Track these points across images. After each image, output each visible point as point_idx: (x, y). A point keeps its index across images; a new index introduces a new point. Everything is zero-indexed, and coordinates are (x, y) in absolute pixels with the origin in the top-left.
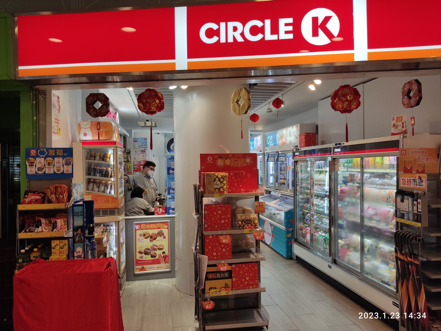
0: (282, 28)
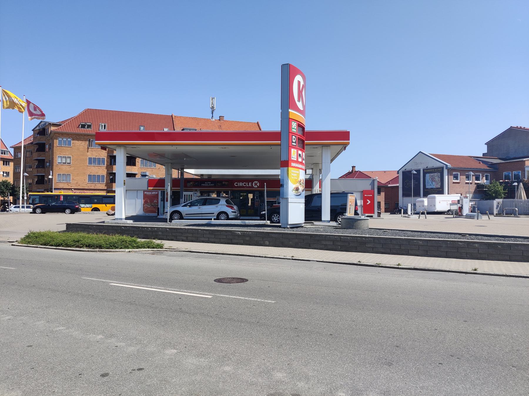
0: (250, 184)
